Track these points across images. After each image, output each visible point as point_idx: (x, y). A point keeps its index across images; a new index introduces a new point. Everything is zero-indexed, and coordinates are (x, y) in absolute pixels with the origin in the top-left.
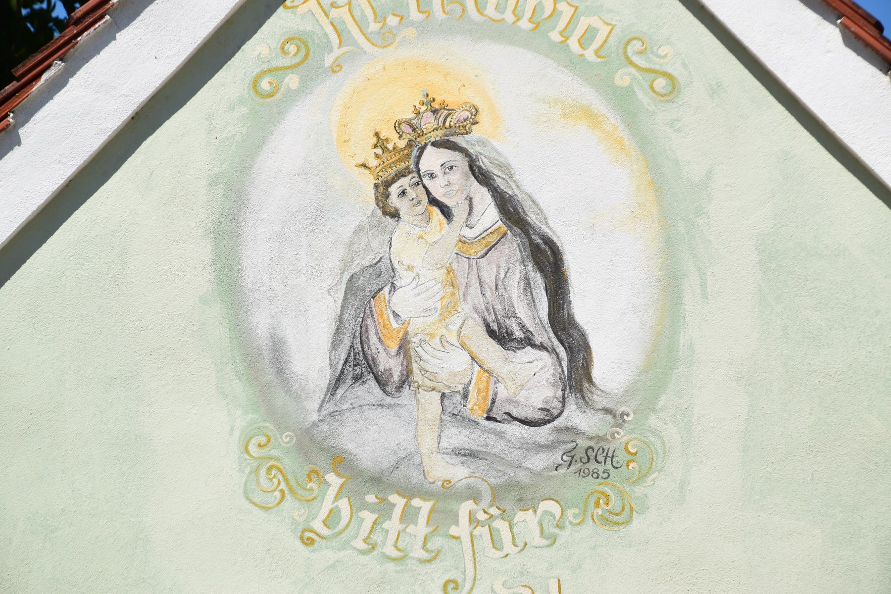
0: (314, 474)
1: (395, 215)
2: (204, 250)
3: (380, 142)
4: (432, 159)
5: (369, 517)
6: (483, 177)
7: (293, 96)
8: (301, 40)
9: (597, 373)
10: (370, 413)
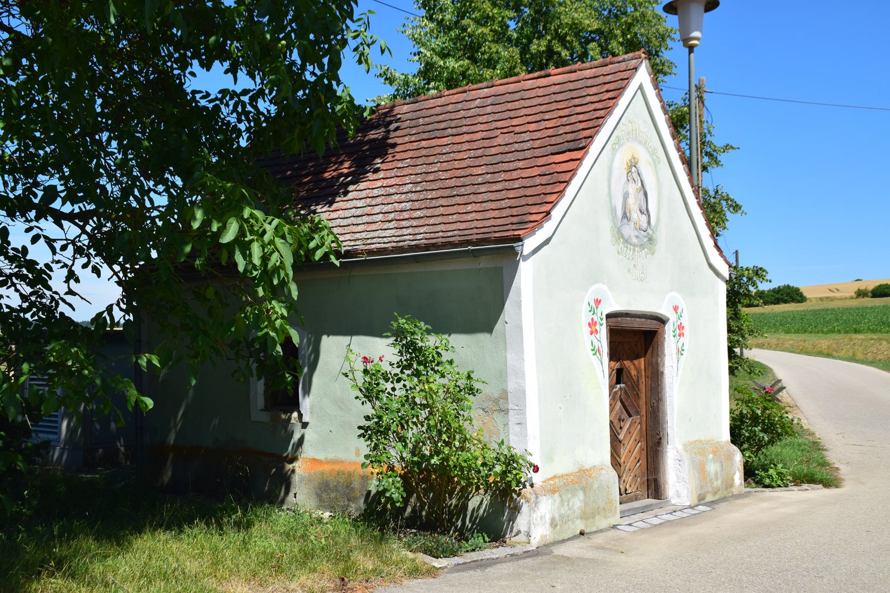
1: (629, 181)
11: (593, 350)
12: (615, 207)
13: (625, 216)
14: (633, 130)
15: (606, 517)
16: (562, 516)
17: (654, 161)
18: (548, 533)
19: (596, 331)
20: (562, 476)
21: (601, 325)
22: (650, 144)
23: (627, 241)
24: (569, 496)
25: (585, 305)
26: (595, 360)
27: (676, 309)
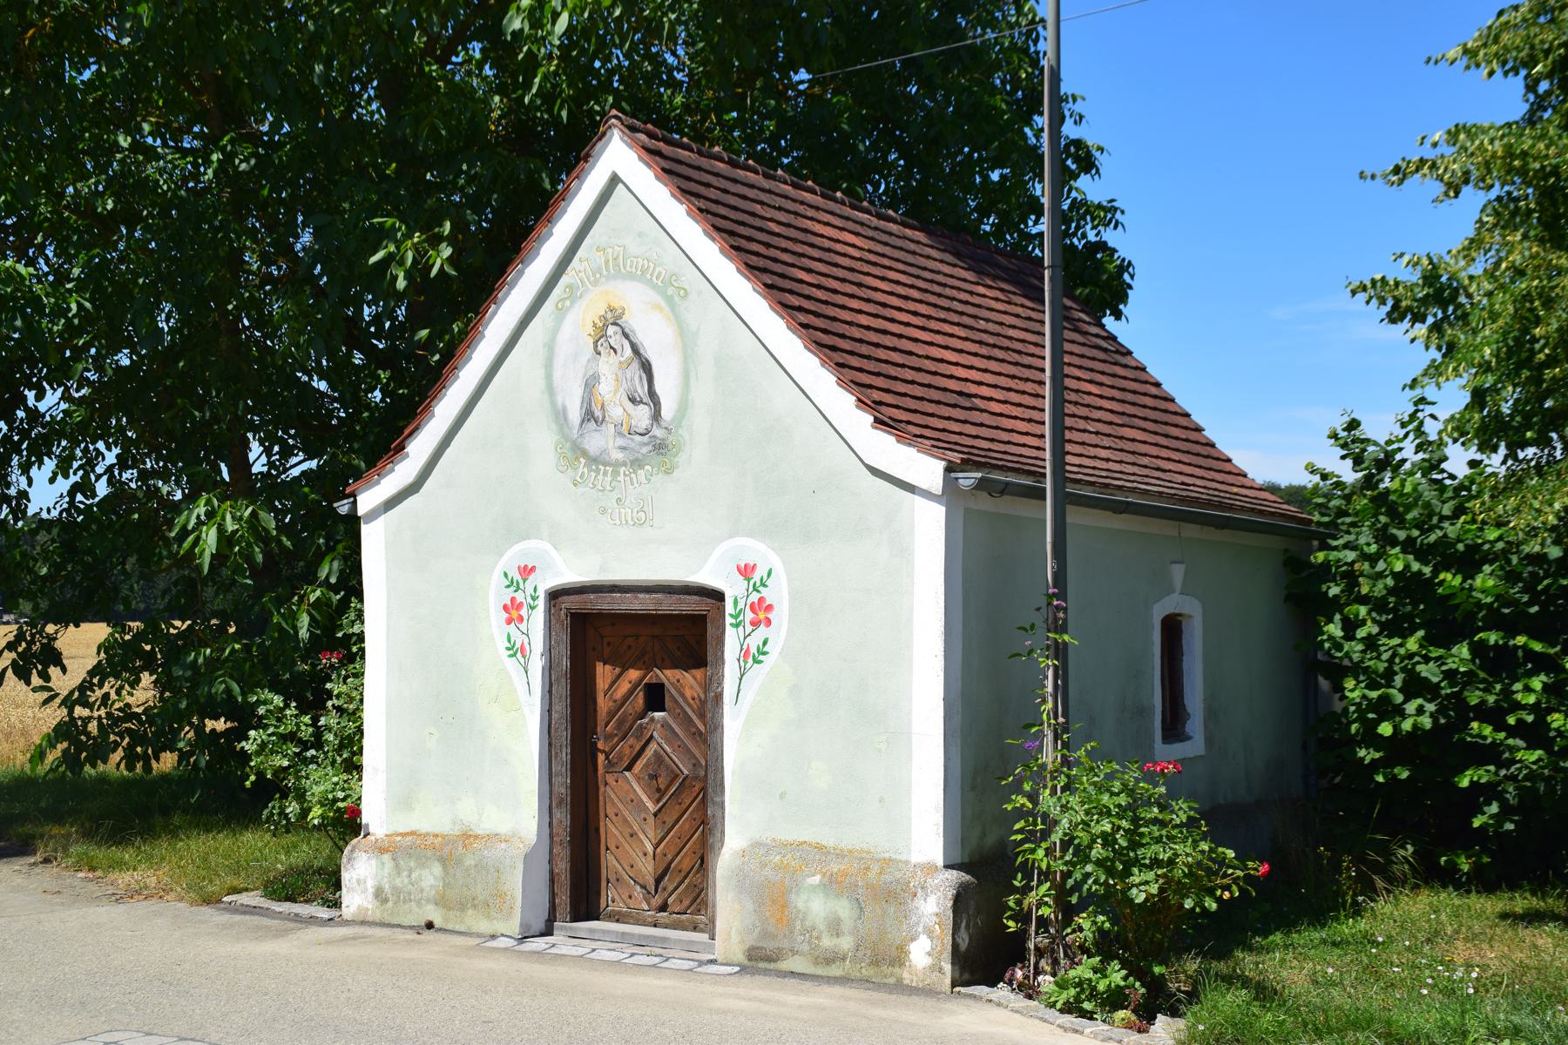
0: (577, 459)
1: (599, 354)
2: (543, 371)
3: (595, 325)
4: (611, 330)
5: (593, 474)
6: (626, 336)
7: (569, 309)
8: (570, 286)
9: (663, 413)
10: (593, 434)
11: (508, 649)
12: (565, 409)
13: (589, 416)
14: (607, 262)
15: (488, 917)
16: (397, 891)
17: (669, 300)
18: (370, 907)
19: (521, 619)
20: (425, 835)
21: (533, 608)
22: (657, 270)
23: (595, 461)
24: (412, 864)
25: (497, 575)
26: (512, 666)
27: (746, 571)
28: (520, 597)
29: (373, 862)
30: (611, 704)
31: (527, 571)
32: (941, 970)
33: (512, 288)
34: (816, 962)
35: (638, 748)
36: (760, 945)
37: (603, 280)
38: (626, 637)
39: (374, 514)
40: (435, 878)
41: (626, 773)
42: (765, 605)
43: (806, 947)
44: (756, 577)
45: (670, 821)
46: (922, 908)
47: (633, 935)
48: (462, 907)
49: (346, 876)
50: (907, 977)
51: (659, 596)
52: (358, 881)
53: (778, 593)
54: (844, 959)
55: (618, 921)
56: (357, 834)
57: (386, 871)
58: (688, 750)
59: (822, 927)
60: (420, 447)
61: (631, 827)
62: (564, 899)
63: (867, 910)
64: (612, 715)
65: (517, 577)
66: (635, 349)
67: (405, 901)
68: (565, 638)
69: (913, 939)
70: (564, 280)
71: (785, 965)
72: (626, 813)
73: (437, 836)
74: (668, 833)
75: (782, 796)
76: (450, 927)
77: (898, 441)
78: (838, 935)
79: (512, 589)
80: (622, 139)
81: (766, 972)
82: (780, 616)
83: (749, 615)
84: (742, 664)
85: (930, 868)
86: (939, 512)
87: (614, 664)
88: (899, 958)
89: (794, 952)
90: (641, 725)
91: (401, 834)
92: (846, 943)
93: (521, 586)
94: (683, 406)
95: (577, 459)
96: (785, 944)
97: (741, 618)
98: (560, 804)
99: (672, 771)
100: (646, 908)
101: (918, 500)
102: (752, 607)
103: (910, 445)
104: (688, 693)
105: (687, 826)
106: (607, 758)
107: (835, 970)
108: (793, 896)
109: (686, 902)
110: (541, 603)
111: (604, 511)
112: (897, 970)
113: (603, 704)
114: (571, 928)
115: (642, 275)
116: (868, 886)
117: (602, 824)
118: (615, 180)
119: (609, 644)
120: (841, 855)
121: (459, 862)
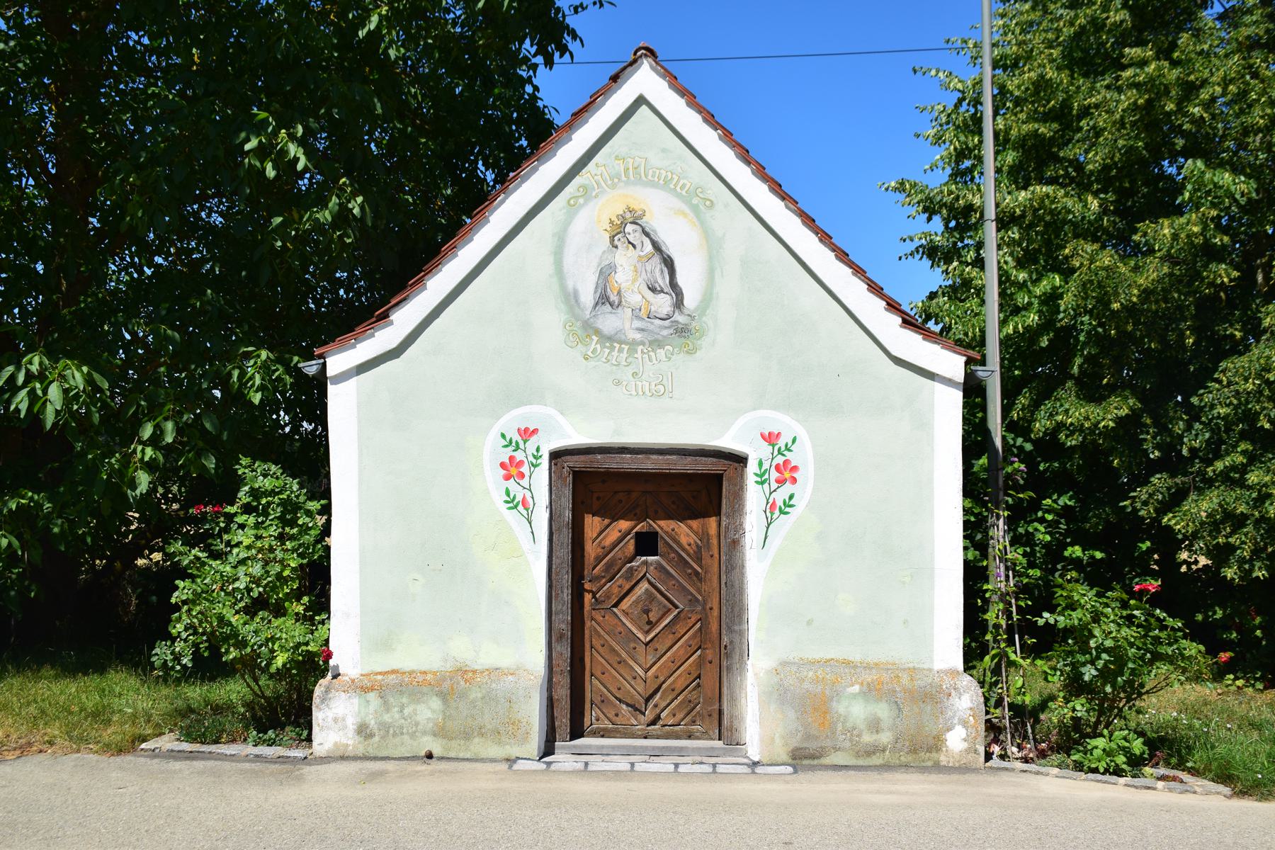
0: (589, 336)
1: (616, 247)
2: (552, 259)
3: (611, 222)
4: (629, 228)
5: (607, 351)
6: (647, 235)
7: (582, 206)
8: (584, 187)
9: (685, 302)
10: (607, 316)
11: (507, 502)
12: (576, 294)
13: (603, 299)
14: (626, 170)
15: (499, 743)
16: (385, 727)
17: (695, 209)
18: (350, 742)
19: (522, 476)
20: (411, 673)
21: (535, 466)
22: (682, 182)
23: (609, 340)
24: (405, 700)
25: (494, 434)
26: (514, 519)
27: (771, 438)
28: (519, 456)
29: (356, 701)
30: (599, 550)
31: (527, 433)
32: (976, 751)
33: (523, 182)
34: (858, 755)
35: (627, 587)
36: (805, 745)
37: (622, 184)
38: (616, 493)
39: (343, 377)
40: (434, 711)
41: (615, 609)
42: (790, 467)
43: (848, 744)
44: (781, 443)
45: (662, 649)
46: (957, 705)
47: (647, 747)
48: (467, 736)
49: (318, 716)
50: (943, 759)
51: (674, 457)
52: (336, 720)
53: (803, 456)
54: (884, 751)
55: (603, 736)
56: (323, 674)
57: (372, 708)
58: (684, 588)
59: (862, 727)
60: (405, 317)
61: (619, 655)
62: (563, 722)
63: (906, 710)
64: (599, 560)
65: (516, 437)
66: (656, 246)
67: (395, 735)
68: (567, 492)
69: (949, 730)
70: (577, 181)
71: (826, 761)
72: (614, 644)
73: (425, 673)
74: (659, 659)
75: (809, 623)
76: (452, 755)
77: (924, 339)
78: (877, 732)
79: (511, 448)
80: (652, 67)
81: (812, 768)
82: (807, 476)
83: (774, 475)
84: (769, 515)
85: (952, 673)
86: (958, 396)
87: (603, 516)
88: (937, 744)
89: (836, 749)
90: (631, 568)
91: (380, 673)
92: (885, 738)
93: (522, 446)
94: (708, 298)
95: (589, 336)
96: (828, 743)
97: (767, 476)
98: (561, 636)
99: (665, 606)
100: (635, 723)
101: (938, 386)
102: (778, 468)
103: (936, 343)
104: (684, 540)
105: (682, 652)
106: (594, 597)
107: (876, 760)
108: (834, 704)
109: (680, 716)
110: (545, 462)
111: (618, 383)
112: (934, 755)
113: (591, 550)
114: (574, 747)
115: (665, 185)
116: (905, 690)
117: (587, 654)
118: (641, 101)
119: (598, 498)
120: (868, 667)
121: (463, 695)
